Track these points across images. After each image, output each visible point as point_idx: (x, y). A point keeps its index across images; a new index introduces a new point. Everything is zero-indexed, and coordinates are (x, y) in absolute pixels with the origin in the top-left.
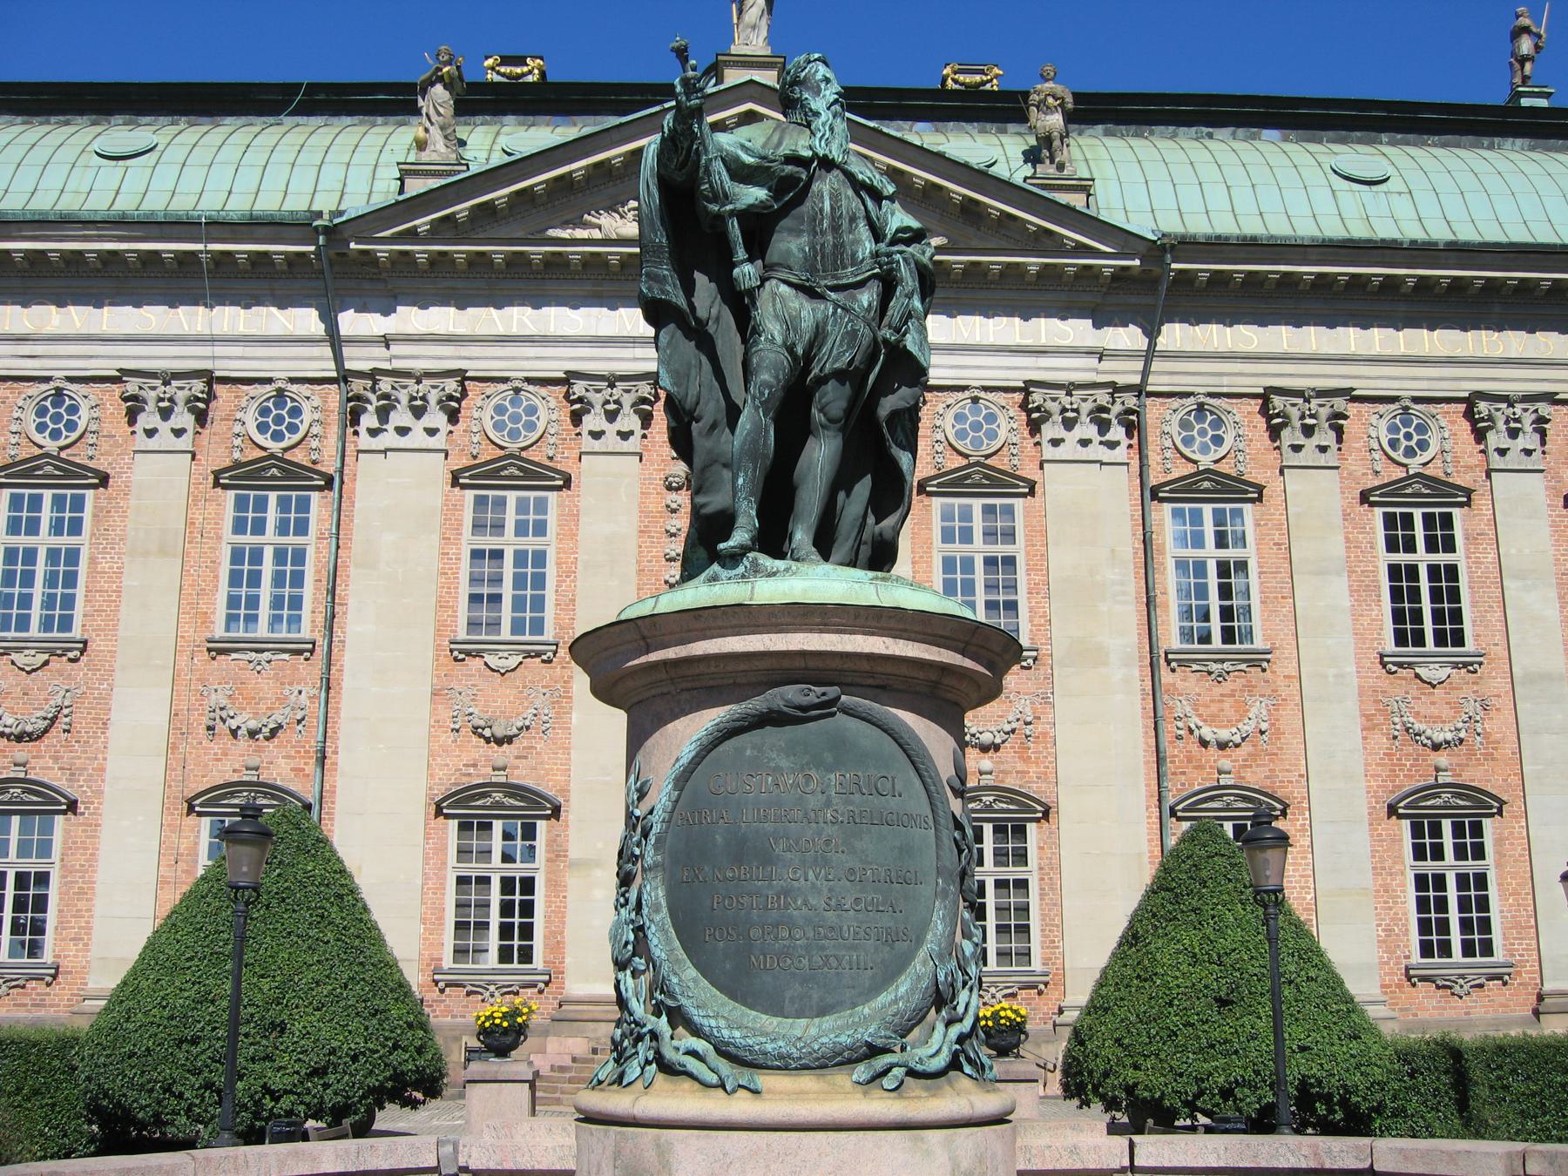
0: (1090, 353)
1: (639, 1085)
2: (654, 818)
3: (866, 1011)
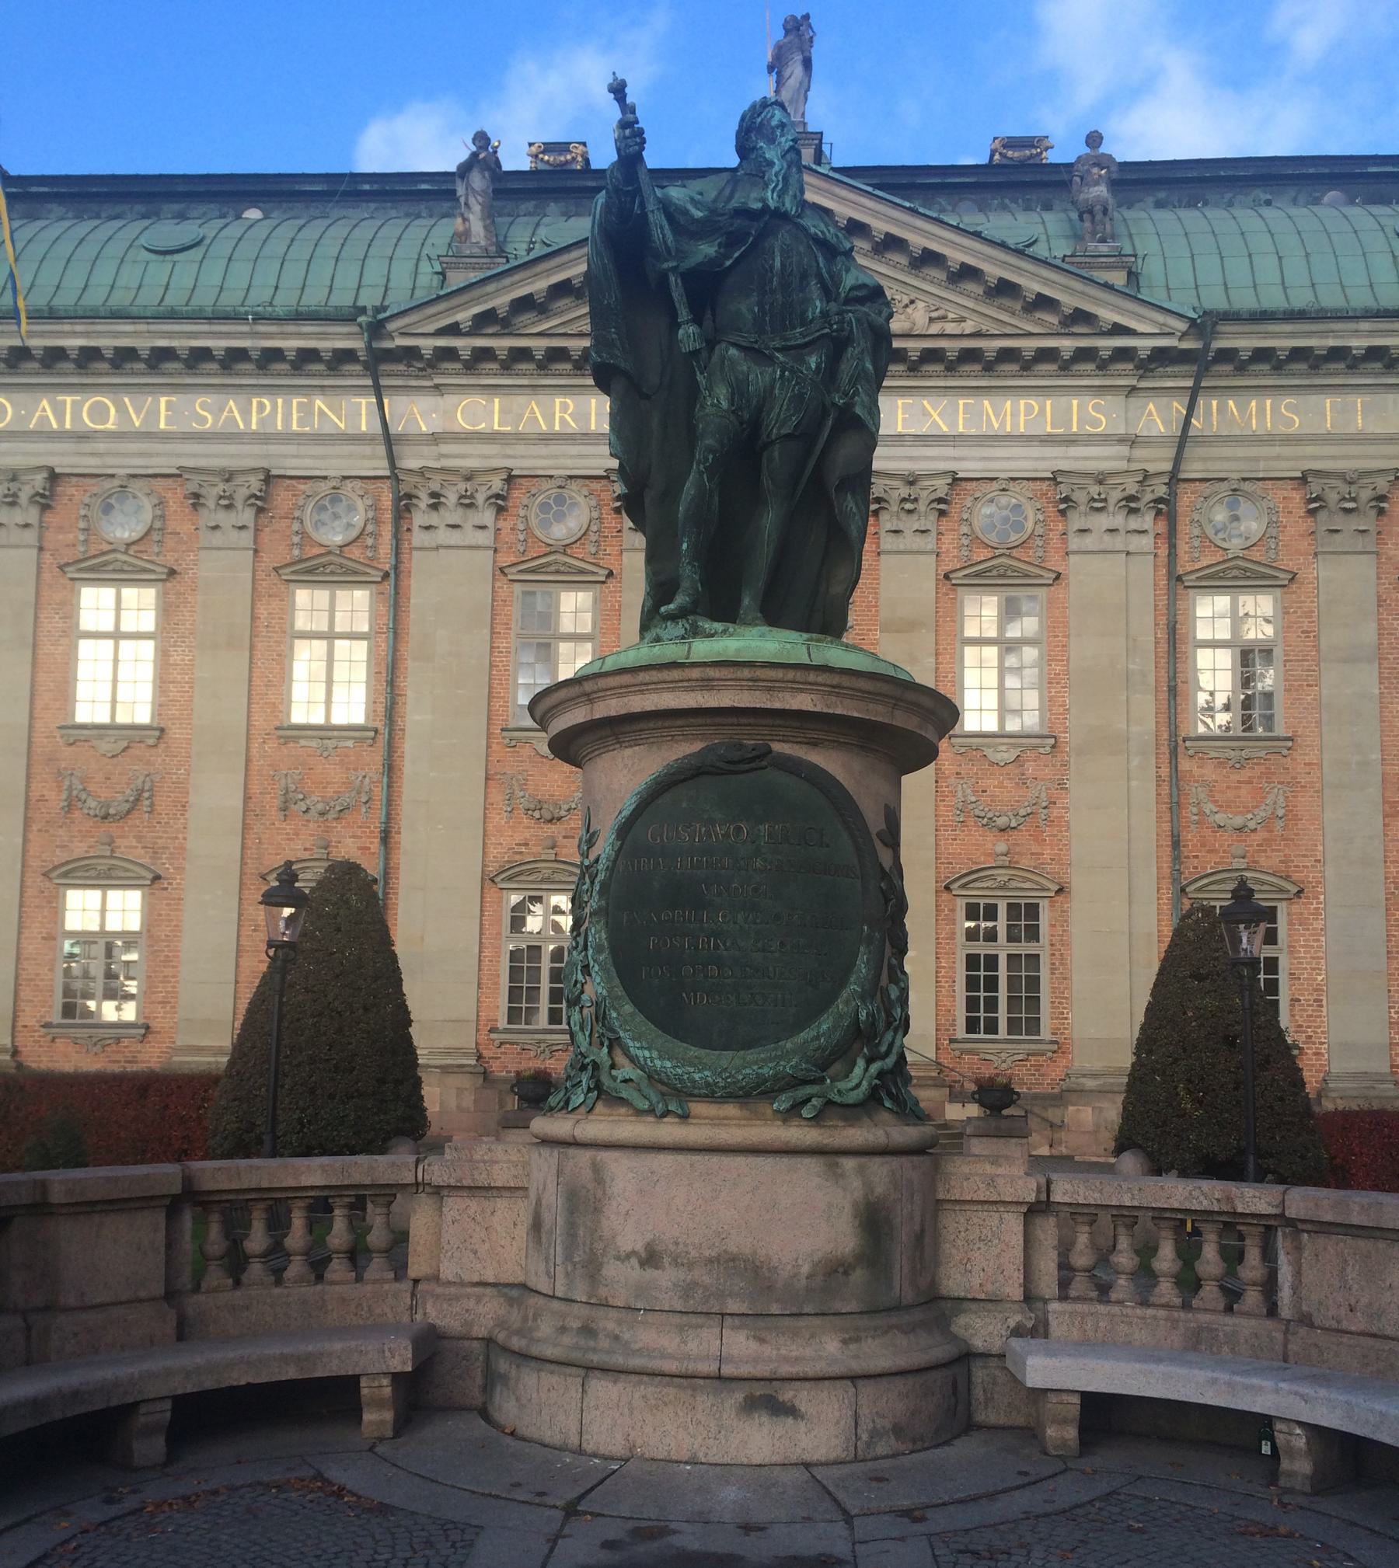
0: (1122, 440)
1: (583, 1110)
2: (600, 866)
3: (789, 1045)
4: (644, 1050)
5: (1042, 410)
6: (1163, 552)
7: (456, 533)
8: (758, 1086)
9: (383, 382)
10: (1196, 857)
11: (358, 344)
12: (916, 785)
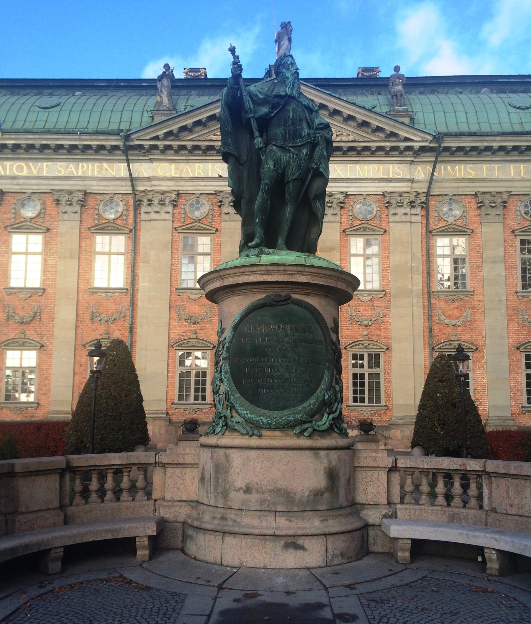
0: (409, 180)
1: (220, 434)
2: (226, 341)
3: (299, 408)
4: (244, 410)
5: (379, 169)
6: (424, 222)
7: (158, 215)
9: (130, 158)
10: (438, 336)
11: (120, 143)
12: (346, 312)
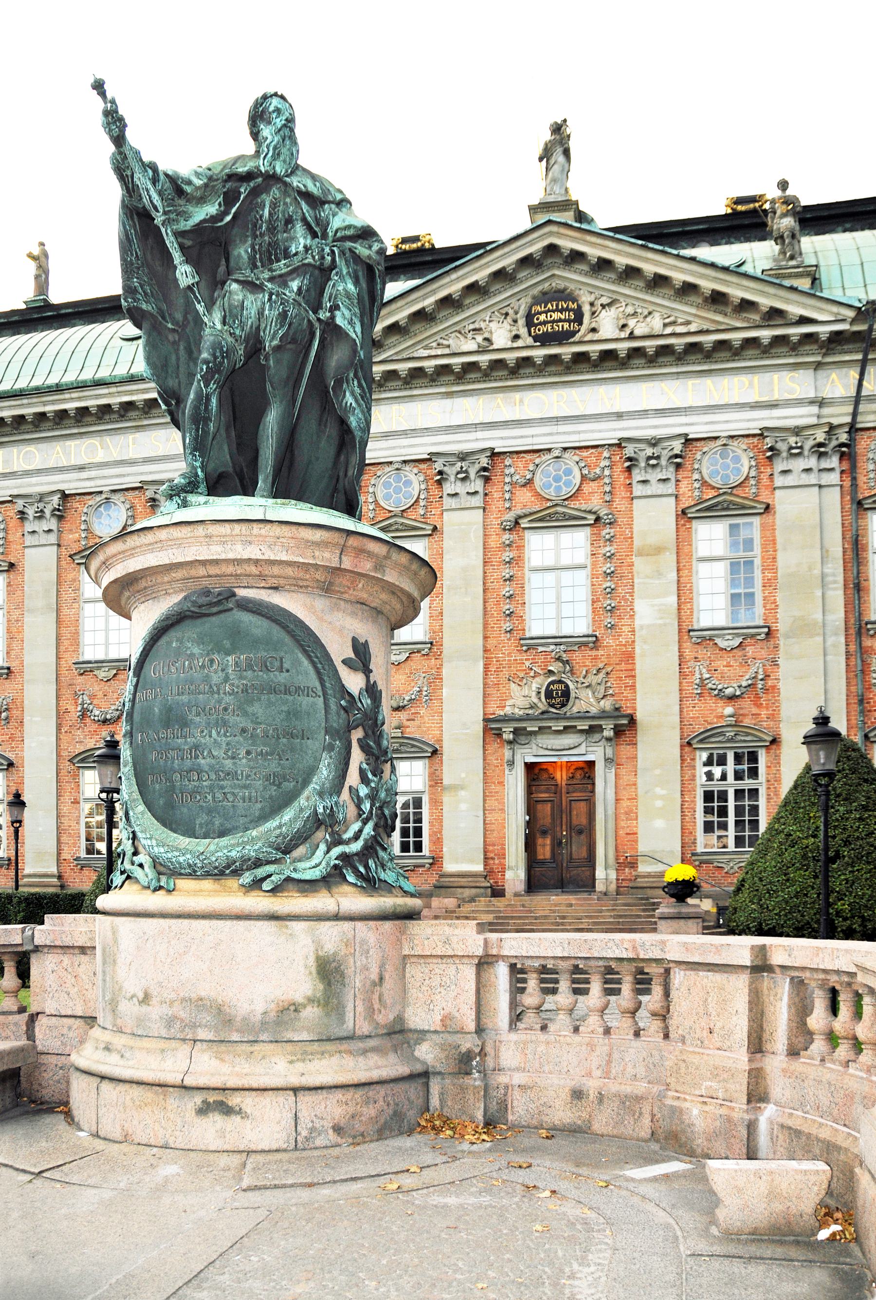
0: (812, 402)
8: (228, 866)
